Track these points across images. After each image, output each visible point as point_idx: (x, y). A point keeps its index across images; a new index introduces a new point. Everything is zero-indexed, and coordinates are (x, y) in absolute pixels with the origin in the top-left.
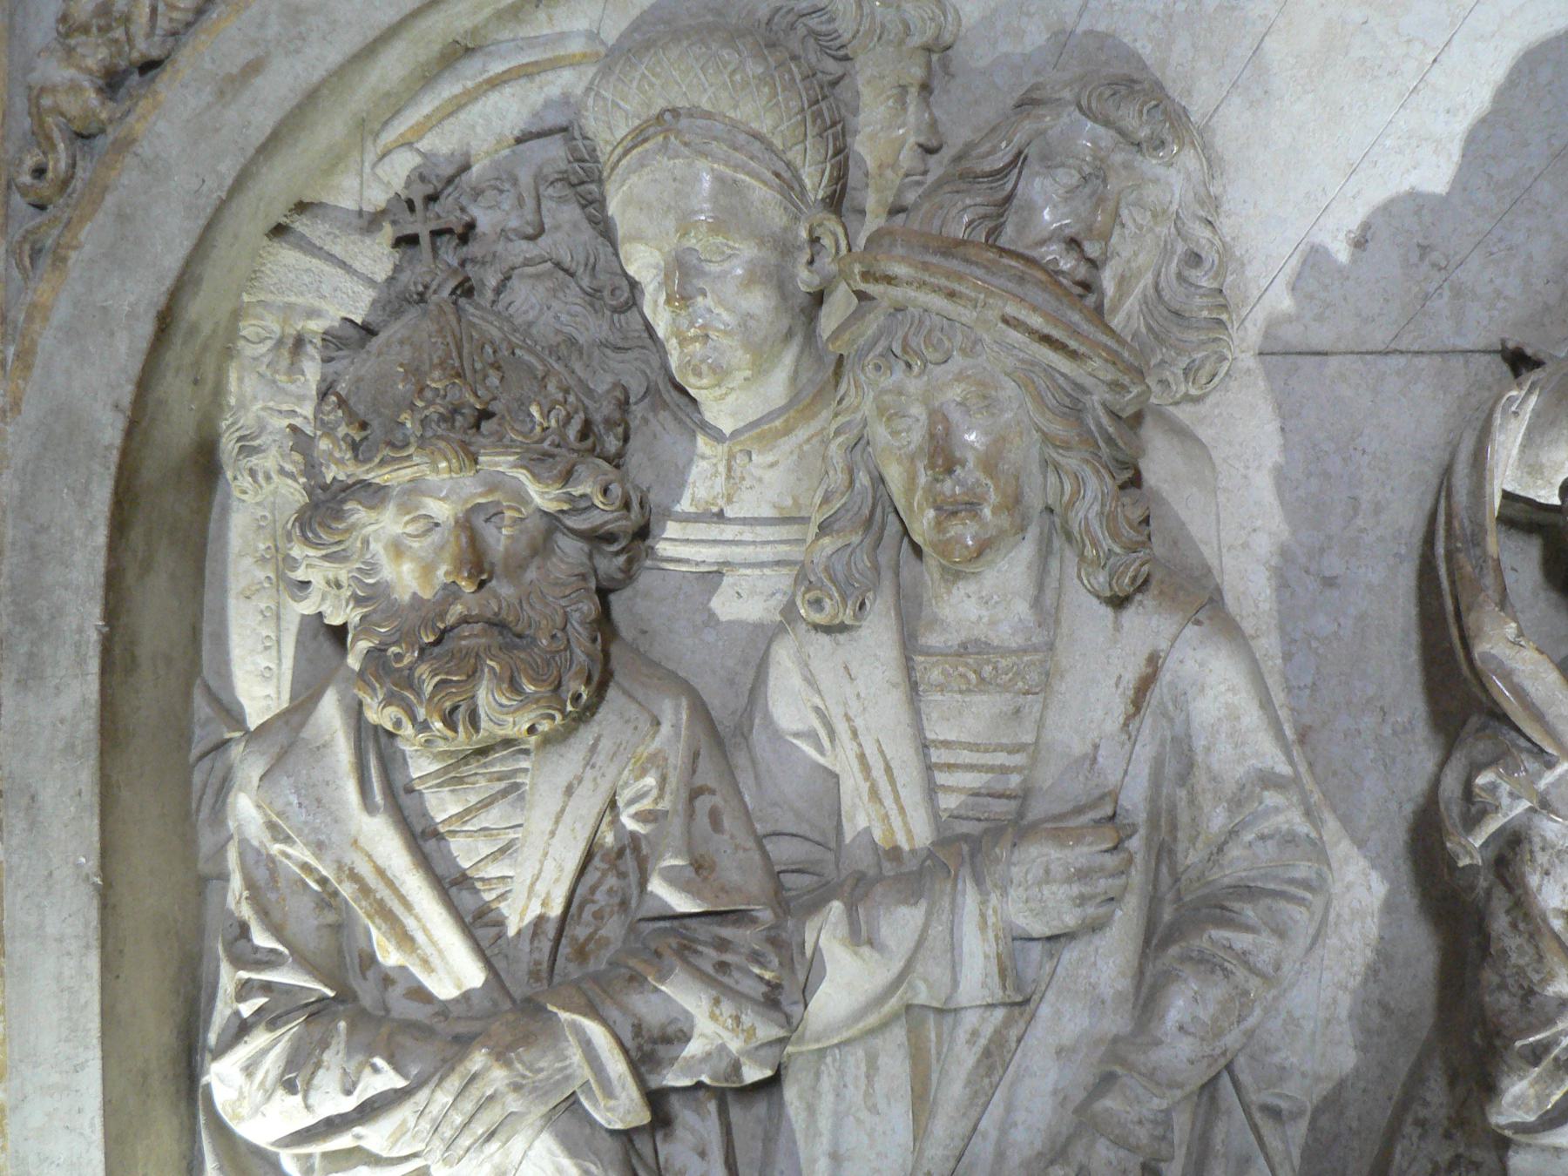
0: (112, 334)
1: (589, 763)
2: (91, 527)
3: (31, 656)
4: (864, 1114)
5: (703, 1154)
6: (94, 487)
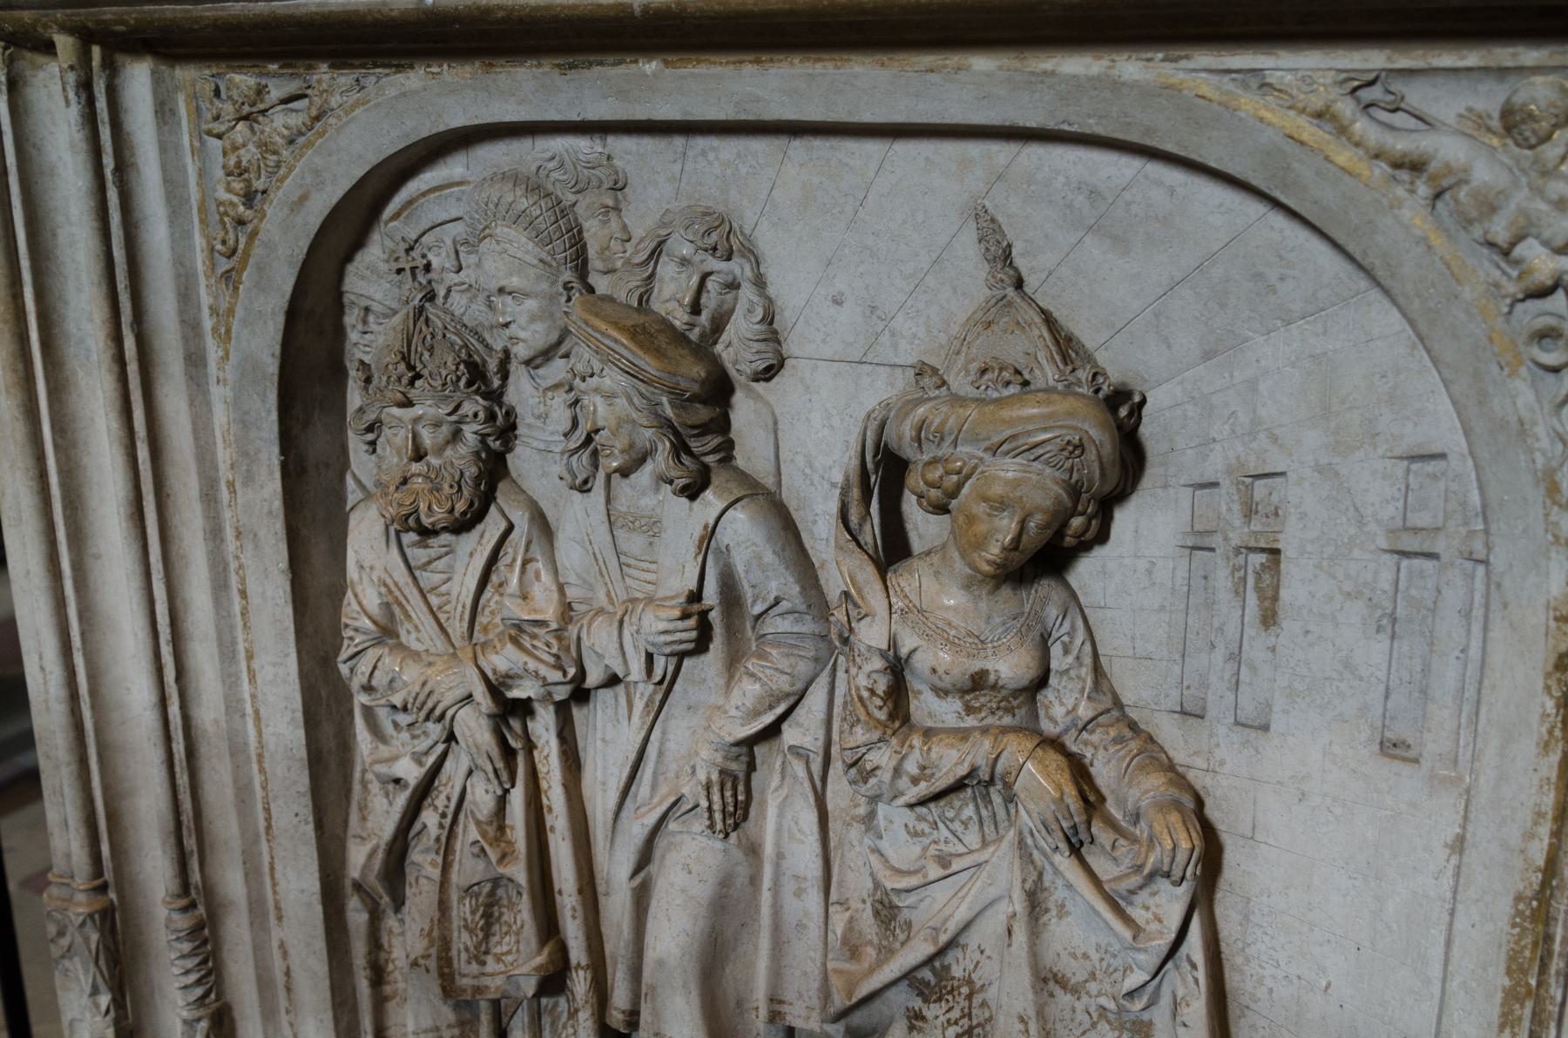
1: (479, 543)
2: (269, 412)
3: (248, 471)
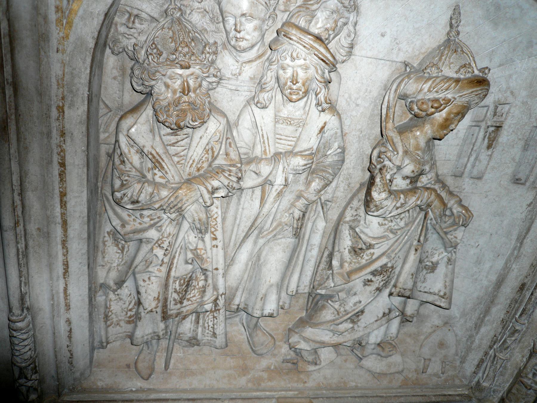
0: (93, 19)
2: (86, 68)
3: (71, 101)
4: (250, 201)
5: (217, 208)
6: (87, 58)
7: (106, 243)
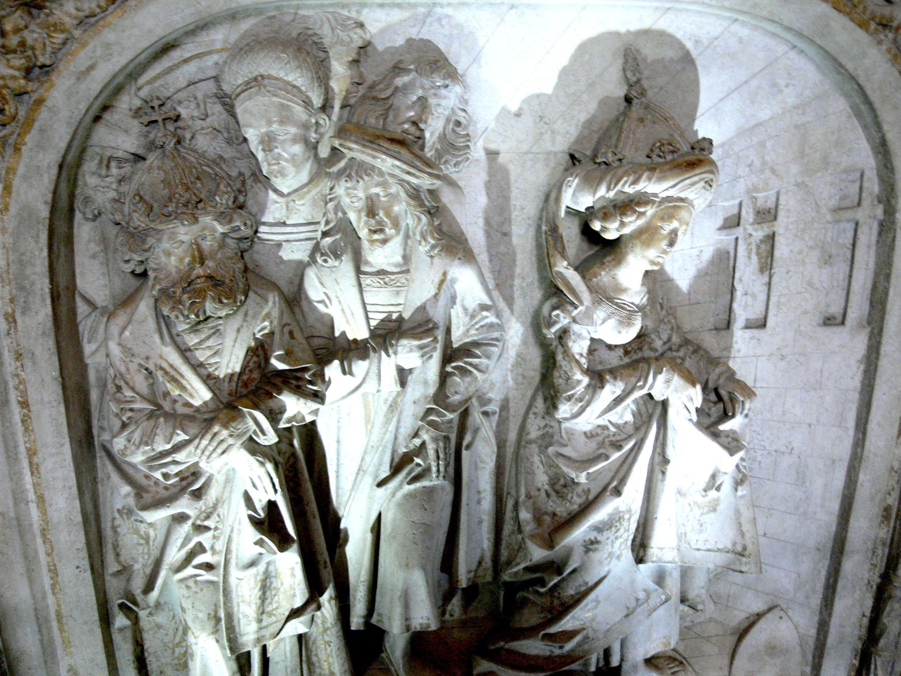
0: (42, 175)
1: (245, 320)
3: (25, 302)
6: (40, 235)
7: (118, 530)
